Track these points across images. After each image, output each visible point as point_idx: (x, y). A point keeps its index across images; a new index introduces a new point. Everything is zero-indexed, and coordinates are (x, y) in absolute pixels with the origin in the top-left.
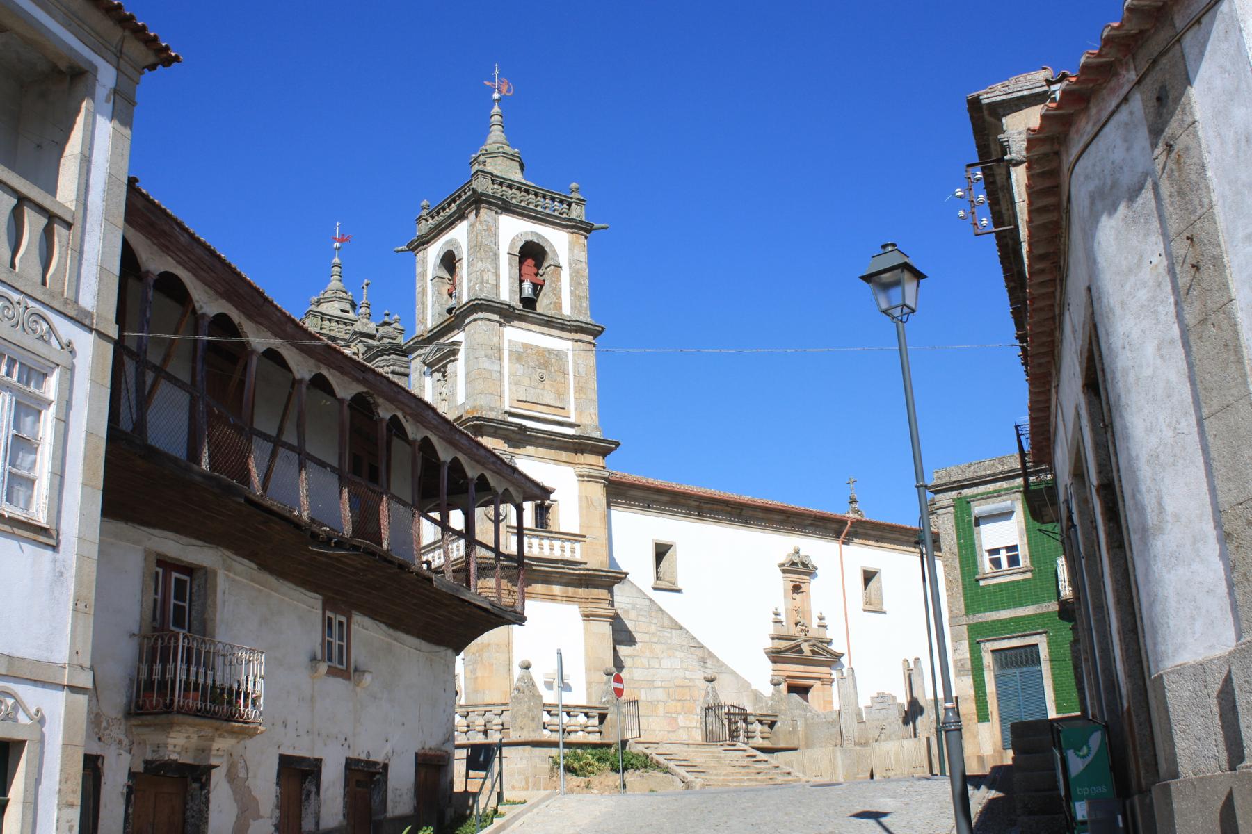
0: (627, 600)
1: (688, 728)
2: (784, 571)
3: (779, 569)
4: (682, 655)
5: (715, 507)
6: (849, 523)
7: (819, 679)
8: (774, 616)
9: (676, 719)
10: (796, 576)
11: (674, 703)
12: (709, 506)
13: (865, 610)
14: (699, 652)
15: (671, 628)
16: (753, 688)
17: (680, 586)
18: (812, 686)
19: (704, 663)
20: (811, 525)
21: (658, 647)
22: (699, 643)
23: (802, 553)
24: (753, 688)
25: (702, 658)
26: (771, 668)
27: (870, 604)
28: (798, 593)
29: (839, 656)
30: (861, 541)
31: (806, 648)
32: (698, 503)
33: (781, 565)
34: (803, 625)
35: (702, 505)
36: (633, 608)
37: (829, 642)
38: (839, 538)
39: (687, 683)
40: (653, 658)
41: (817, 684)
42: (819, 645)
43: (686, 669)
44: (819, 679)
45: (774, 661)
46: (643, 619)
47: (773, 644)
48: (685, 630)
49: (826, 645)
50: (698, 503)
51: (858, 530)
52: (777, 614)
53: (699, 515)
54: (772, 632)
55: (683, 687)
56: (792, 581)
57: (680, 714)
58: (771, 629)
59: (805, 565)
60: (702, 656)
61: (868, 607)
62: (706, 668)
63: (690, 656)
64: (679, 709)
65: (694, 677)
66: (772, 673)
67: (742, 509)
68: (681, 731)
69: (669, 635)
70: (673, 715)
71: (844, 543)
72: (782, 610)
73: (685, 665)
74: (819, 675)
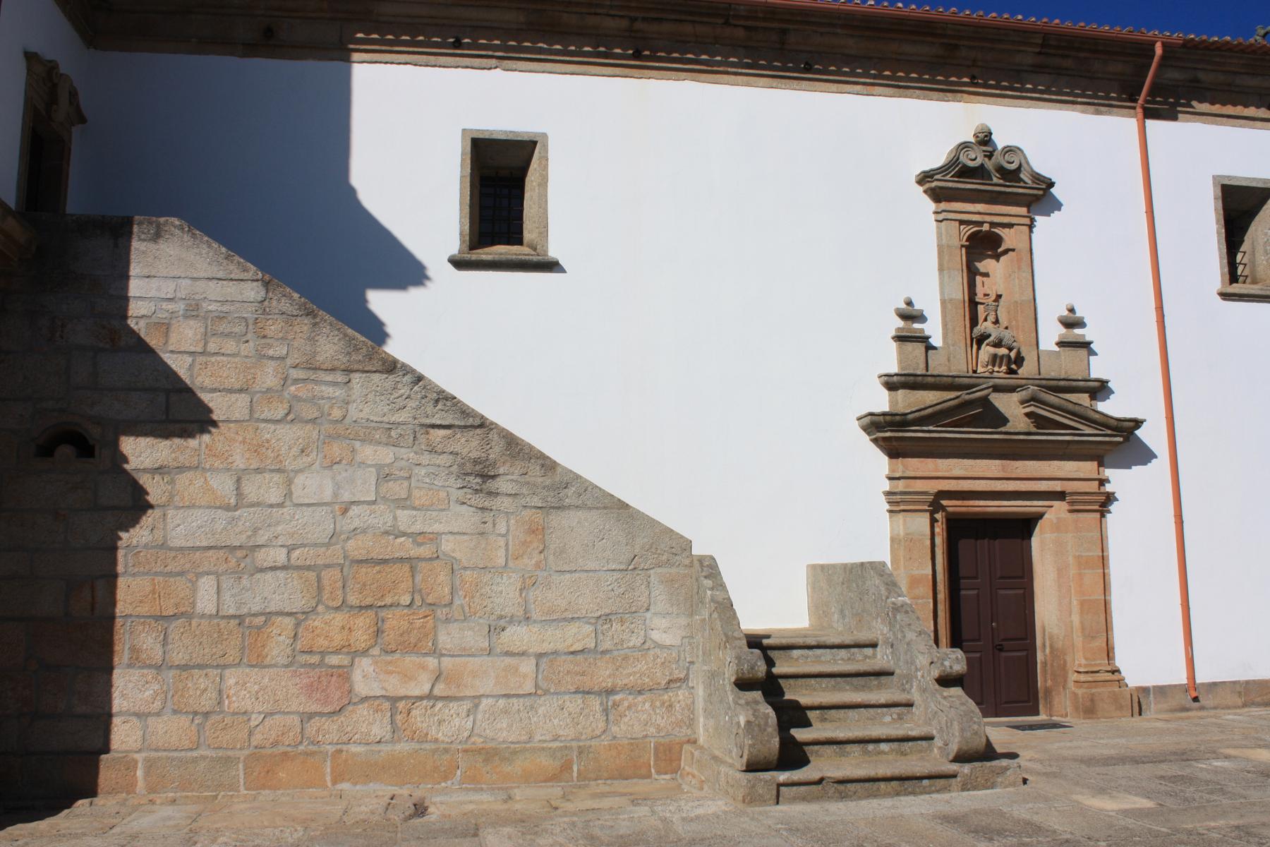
0: (168, 289)
1: (394, 700)
2: (937, 195)
3: (921, 189)
4: (386, 455)
5: (688, 28)
6: (1159, 50)
7: (1061, 496)
8: (900, 323)
9: (344, 674)
10: (980, 207)
11: (339, 618)
12: (666, 27)
13: (1225, 296)
14: (468, 445)
15: (348, 371)
16: (696, 551)
17: (553, 253)
18: (1040, 516)
19: (486, 477)
20: (1038, 69)
21: (288, 436)
22: (465, 412)
23: (1000, 141)
24: (696, 551)
25: (476, 462)
26: (886, 472)
27: (1254, 282)
28: (997, 257)
29: (1128, 428)
30: (1217, 108)
31: (1011, 406)
32: (624, 23)
33: (924, 178)
34: (998, 344)
35: (639, 25)
36: (193, 310)
37: (1100, 389)
38: (1135, 101)
39: (404, 547)
40: (258, 471)
41: (1056, 512)
42: (1051, 398)
43: (403, 503)
44: (1061, 496)
45: (894, 450)
46: (230, 346)
47: (892, 402)
48: (407, 370)
49: (1084, 399)
50: (624, 23)
51: (1201, 75)
52: (910, 315)
53: (637, 55)
54: (894, 368)
55: (384, 562)
56: (962, 222)
57: (365, 652)
58: (890, 360)
59: (1012, 175)
60: (474, 455)
61: (1236, 288)
62: (492, 494)
63: (426, 458)
64: (361, 637)
65: (437, 527)
66: (887, 485)
67: (784, 32)
68: (363, 711)
69: (339, 393)
70: (334, 660)
71: (1150, 114)
72: (930, 304)
73: (397, 489)
74: (1057, 486)
